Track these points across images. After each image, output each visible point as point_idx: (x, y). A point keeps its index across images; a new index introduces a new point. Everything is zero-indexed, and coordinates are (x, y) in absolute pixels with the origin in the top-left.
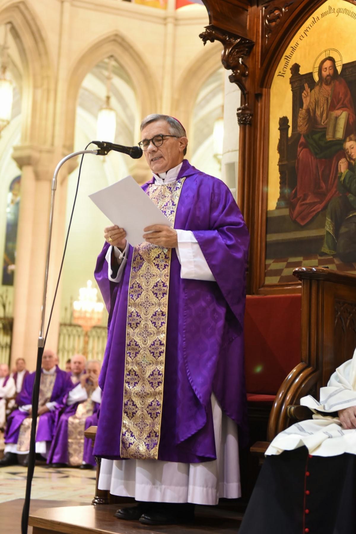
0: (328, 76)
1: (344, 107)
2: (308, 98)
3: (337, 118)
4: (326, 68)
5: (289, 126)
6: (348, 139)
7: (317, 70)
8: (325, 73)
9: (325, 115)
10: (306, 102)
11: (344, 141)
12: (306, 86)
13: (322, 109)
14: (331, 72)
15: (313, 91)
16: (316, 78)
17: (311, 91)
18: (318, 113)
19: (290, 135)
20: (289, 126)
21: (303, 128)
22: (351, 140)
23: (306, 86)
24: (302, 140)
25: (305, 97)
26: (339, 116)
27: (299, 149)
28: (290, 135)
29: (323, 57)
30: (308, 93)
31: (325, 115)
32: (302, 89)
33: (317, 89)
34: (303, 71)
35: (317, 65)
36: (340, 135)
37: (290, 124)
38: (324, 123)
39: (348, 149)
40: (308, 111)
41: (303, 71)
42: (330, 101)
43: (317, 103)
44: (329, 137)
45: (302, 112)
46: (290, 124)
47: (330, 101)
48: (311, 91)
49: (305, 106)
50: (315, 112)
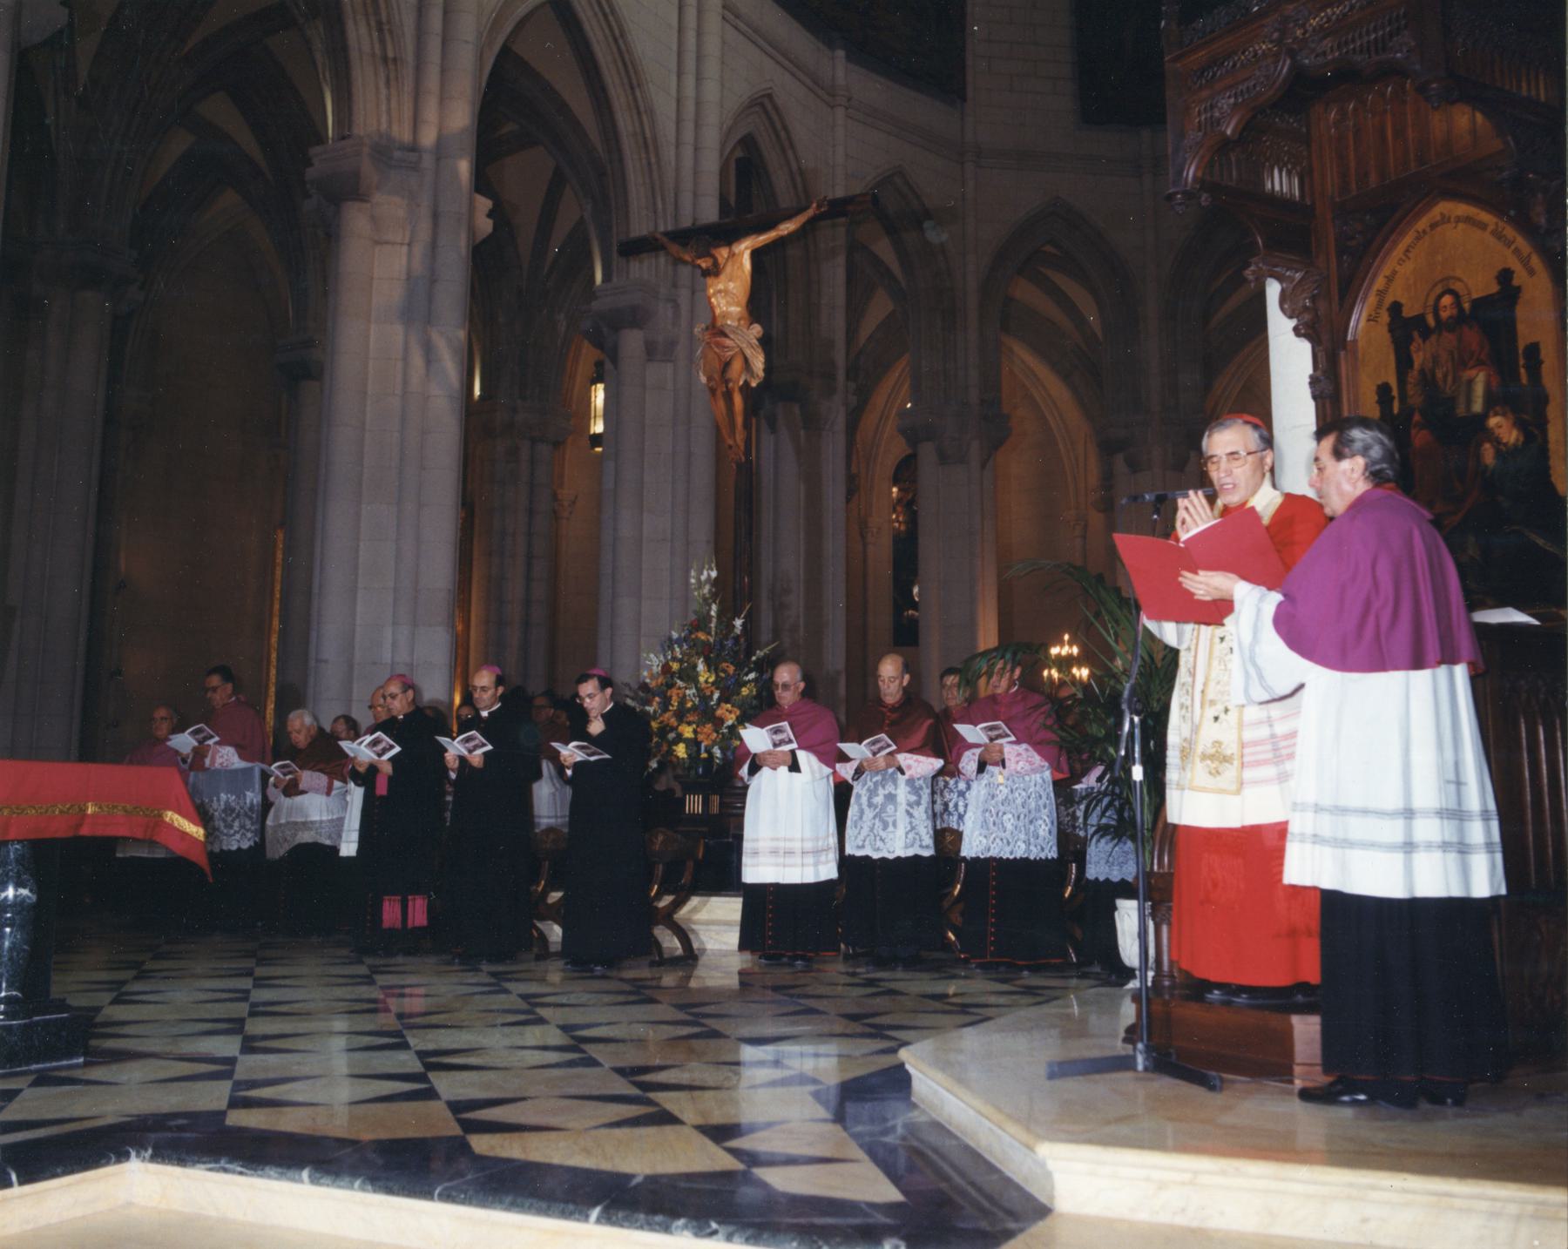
0: (1451, 317)
1: (1480, 364)
2: (1421, 354)
3: (1470, 382)
4: (1445, 307)
5: (1393, 398)
6: (1491, 413)
7: (1430, 310)
8: (1444, 315)
9: (1450, 379)
10: (1418, 359)
11: (1484, 417)
12: (1416, 334)
13: (1445, 369)
14: (1455, 312)
15: (1428, 342)
16: (1431, 321)
17: (1424, 341)
18: (1439, 375)
19: (1396, 410)
20: (1393, 398)
21: (1416, 398)
22: (1496, 414)
23: (1416, 334)
24: (1417, 417)
25: (1419, 350)
26: (1475, 378)
27: (1413, 431)
28: (1396, 410)
29: (1439, 290)
30: (1419, 345)
31: (1450, 379)
32: (1410, 340)
33: (1433, 338)
34: (1407, 312)
35: (1431, 302)
36: (1478, 407)
37: (1395, 393)
38: (1450, 389)
39: (1492, 429)
40: (1422, 371)
41: (1407, 312)
42: (1456, 356)
43: (1435, 359)
44: (1461, 411)
45: (1413, 376)
46: (1395, 393)
47: (1456, 356)
48: (1424, 341)
49: (1417, 365)
50: (1434, 375)
